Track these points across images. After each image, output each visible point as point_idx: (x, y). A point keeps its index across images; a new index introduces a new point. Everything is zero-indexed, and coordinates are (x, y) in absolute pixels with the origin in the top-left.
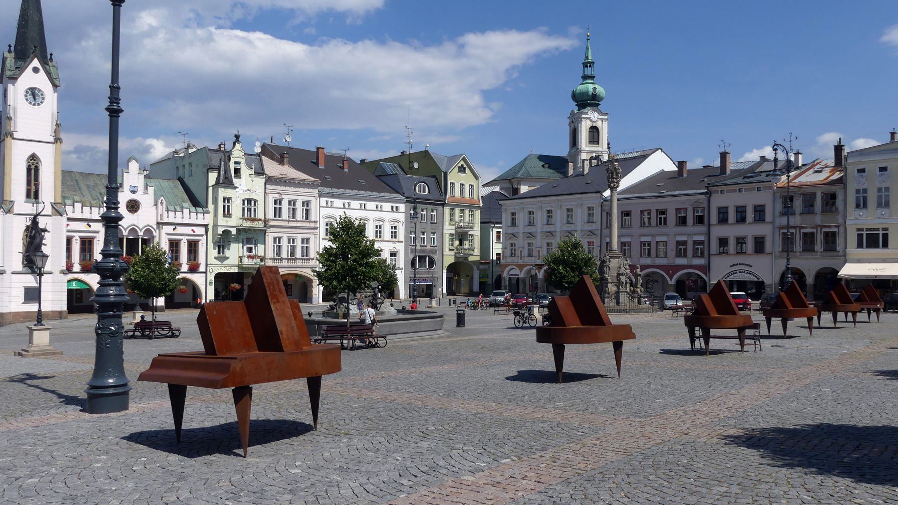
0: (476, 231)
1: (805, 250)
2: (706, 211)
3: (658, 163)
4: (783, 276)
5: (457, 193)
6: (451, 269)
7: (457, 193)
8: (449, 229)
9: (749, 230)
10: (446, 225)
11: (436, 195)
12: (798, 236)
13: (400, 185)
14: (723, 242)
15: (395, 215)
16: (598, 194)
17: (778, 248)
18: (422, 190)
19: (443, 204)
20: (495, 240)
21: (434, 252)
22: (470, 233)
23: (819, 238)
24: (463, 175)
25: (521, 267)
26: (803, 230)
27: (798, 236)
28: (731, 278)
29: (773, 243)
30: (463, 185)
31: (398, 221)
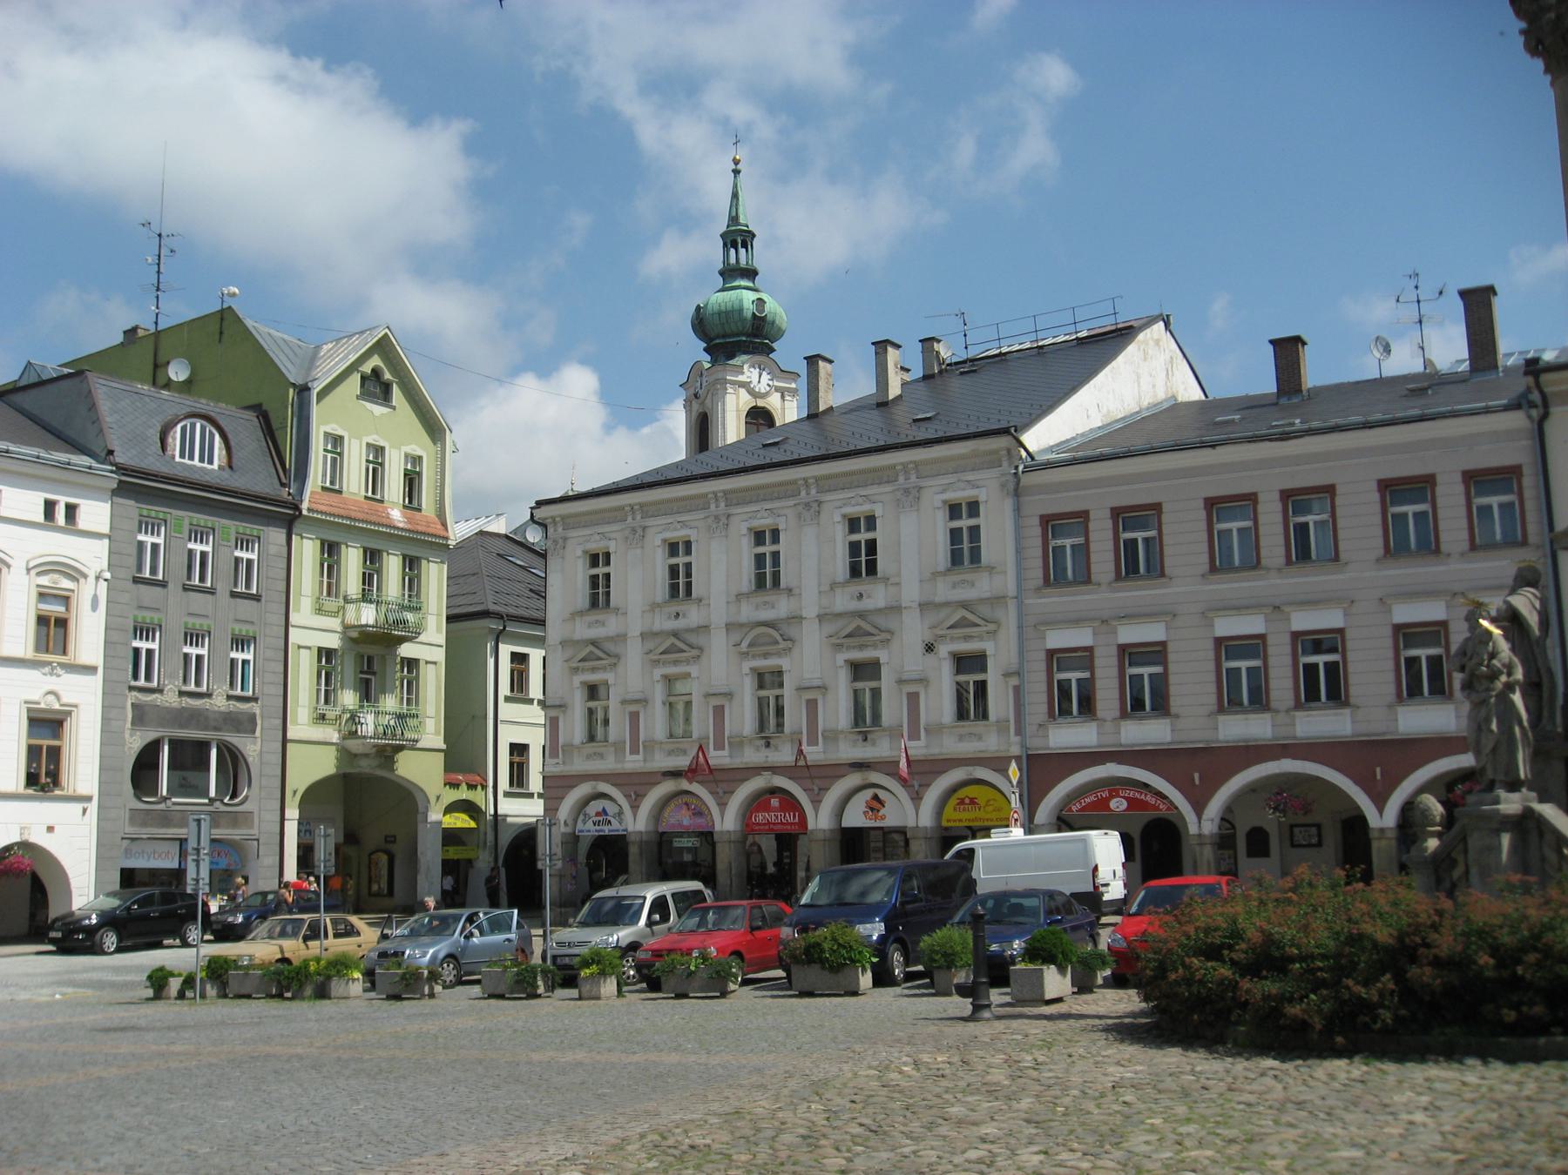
0: (429, 645)
3: (1144, 379)
5: (354, 481)
6: (314, 795)
7: (354, 481)
8: (314, 629)
10: (302, 612)
11: (259, 479)
13: (96, 420)
15: (57, 545)
16: (1002, 442)
18: (200, 455)
19: (289, 517)
20: (505, 689)
21: (246, 724)
22: (406, 650)
24: (378, 410)
25: (636, 785)
30: (379, 451)
31: (75, 574)
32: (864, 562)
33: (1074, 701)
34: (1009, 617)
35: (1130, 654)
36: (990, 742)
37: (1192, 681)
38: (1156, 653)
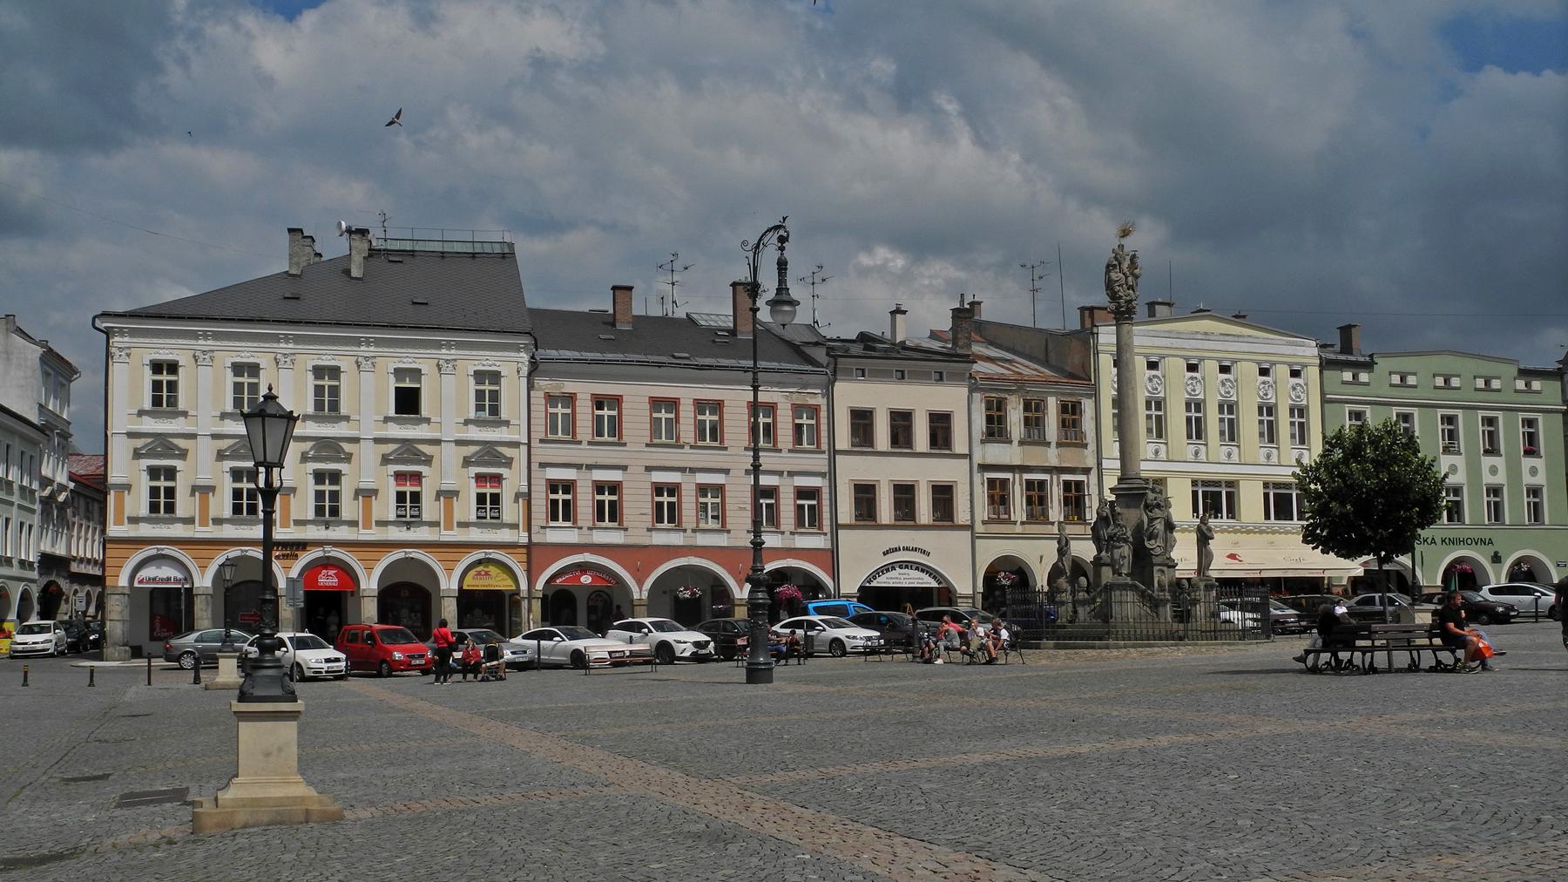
1: (1032, 518)
2: (823, 414)
4: (990, 578)
9: (924, 472)
12: (1017, 487)
14: (865, 495)
17: (983, 511)
23: (1056, 494)
26: (1026, 476)
27: (1017, 487)
28: (883, 581)
29: (970, 503)
32: (408, 402)
33: (563, 511)
34: (520, 455)
35: (599, 487)
36: (505, 536)
37: (637, 505)
38: (614, 488)
